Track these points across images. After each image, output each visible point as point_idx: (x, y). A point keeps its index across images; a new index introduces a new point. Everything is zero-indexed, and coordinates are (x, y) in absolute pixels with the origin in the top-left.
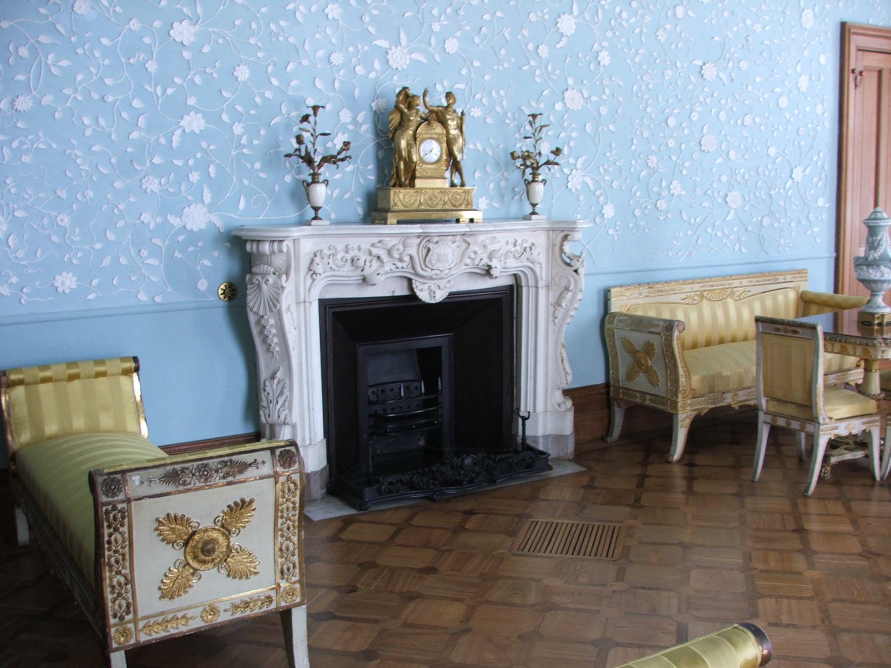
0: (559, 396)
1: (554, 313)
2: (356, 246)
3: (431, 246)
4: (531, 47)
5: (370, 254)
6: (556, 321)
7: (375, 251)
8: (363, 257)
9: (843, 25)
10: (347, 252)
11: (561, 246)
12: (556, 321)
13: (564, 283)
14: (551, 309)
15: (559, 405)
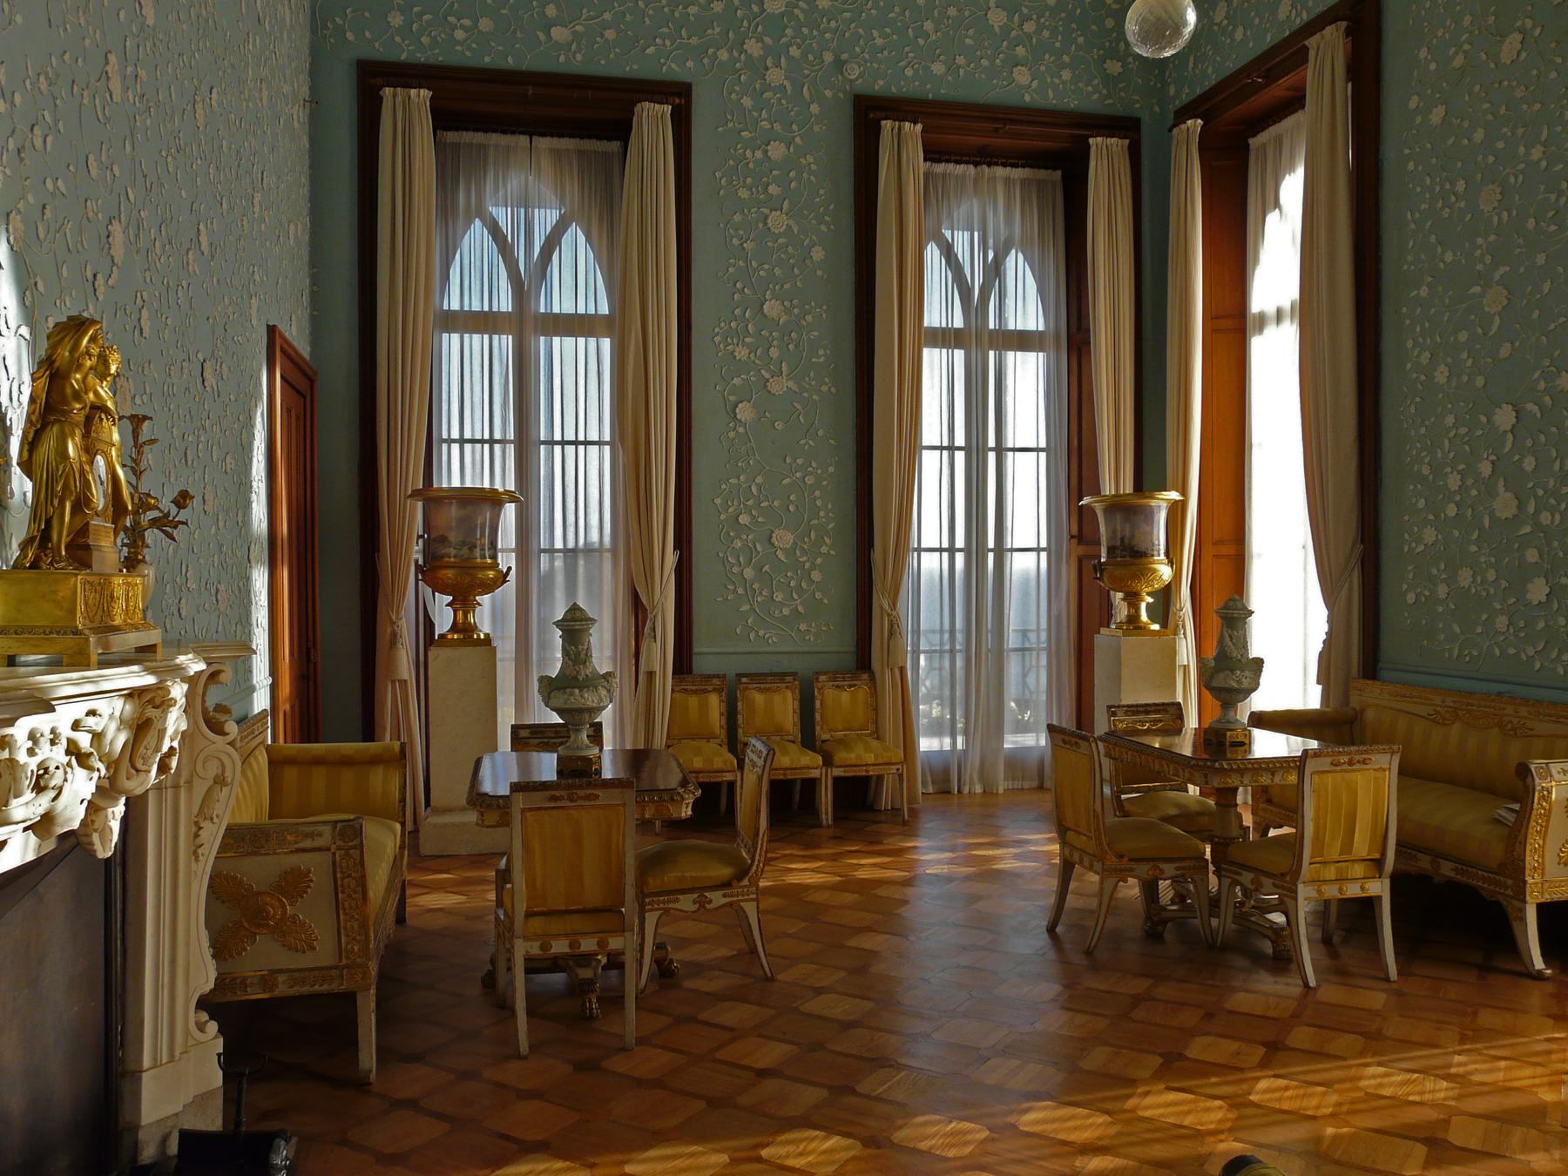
0: (188, 1014)
1: (197, 836)
2: (47, 732)
3: (151, 712)
4: (89, 274)
5: (73, 749)
6: (200, 851)
7: (84, 740)
8: (58, 755)
9: (272, 331)
10: (31, 752)
11: (204, 694)
12: (200, 851)
13: (213, 770)
14: (194, 829)
15: (201, 1027)
